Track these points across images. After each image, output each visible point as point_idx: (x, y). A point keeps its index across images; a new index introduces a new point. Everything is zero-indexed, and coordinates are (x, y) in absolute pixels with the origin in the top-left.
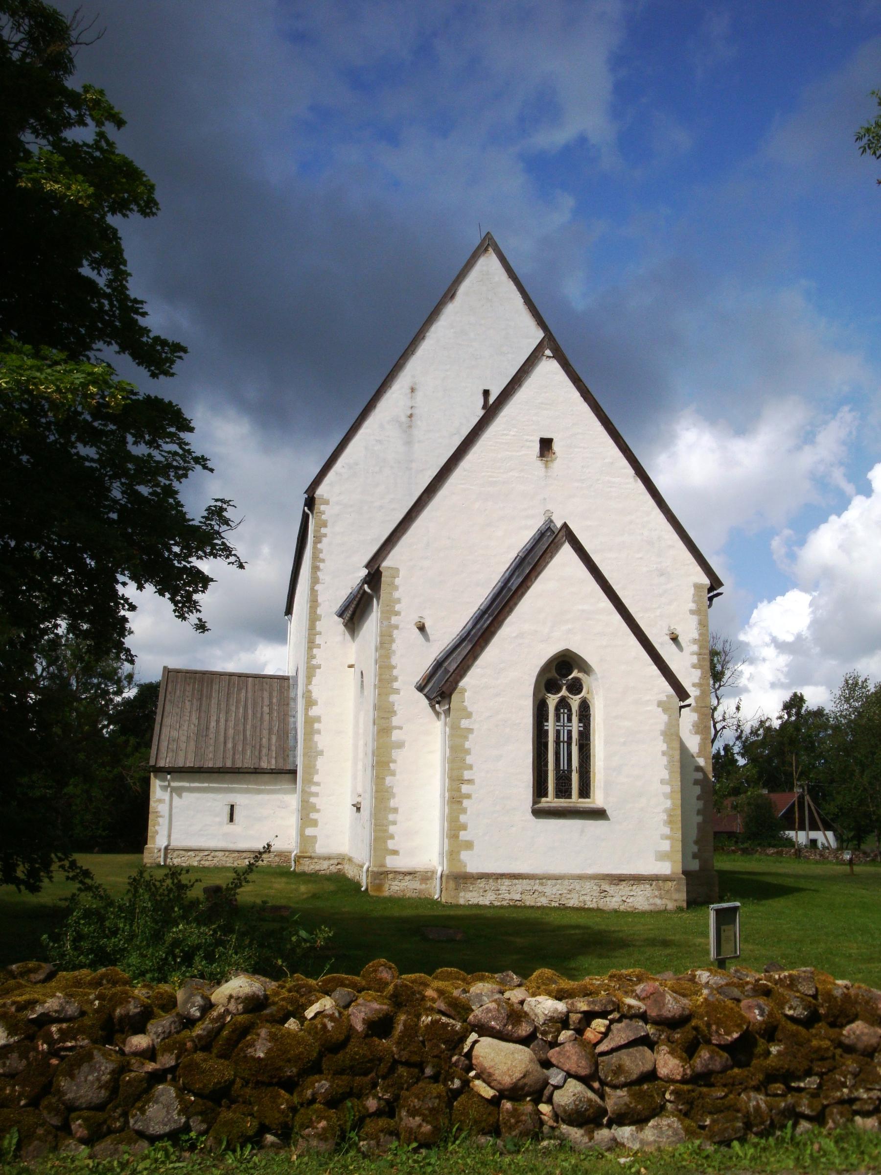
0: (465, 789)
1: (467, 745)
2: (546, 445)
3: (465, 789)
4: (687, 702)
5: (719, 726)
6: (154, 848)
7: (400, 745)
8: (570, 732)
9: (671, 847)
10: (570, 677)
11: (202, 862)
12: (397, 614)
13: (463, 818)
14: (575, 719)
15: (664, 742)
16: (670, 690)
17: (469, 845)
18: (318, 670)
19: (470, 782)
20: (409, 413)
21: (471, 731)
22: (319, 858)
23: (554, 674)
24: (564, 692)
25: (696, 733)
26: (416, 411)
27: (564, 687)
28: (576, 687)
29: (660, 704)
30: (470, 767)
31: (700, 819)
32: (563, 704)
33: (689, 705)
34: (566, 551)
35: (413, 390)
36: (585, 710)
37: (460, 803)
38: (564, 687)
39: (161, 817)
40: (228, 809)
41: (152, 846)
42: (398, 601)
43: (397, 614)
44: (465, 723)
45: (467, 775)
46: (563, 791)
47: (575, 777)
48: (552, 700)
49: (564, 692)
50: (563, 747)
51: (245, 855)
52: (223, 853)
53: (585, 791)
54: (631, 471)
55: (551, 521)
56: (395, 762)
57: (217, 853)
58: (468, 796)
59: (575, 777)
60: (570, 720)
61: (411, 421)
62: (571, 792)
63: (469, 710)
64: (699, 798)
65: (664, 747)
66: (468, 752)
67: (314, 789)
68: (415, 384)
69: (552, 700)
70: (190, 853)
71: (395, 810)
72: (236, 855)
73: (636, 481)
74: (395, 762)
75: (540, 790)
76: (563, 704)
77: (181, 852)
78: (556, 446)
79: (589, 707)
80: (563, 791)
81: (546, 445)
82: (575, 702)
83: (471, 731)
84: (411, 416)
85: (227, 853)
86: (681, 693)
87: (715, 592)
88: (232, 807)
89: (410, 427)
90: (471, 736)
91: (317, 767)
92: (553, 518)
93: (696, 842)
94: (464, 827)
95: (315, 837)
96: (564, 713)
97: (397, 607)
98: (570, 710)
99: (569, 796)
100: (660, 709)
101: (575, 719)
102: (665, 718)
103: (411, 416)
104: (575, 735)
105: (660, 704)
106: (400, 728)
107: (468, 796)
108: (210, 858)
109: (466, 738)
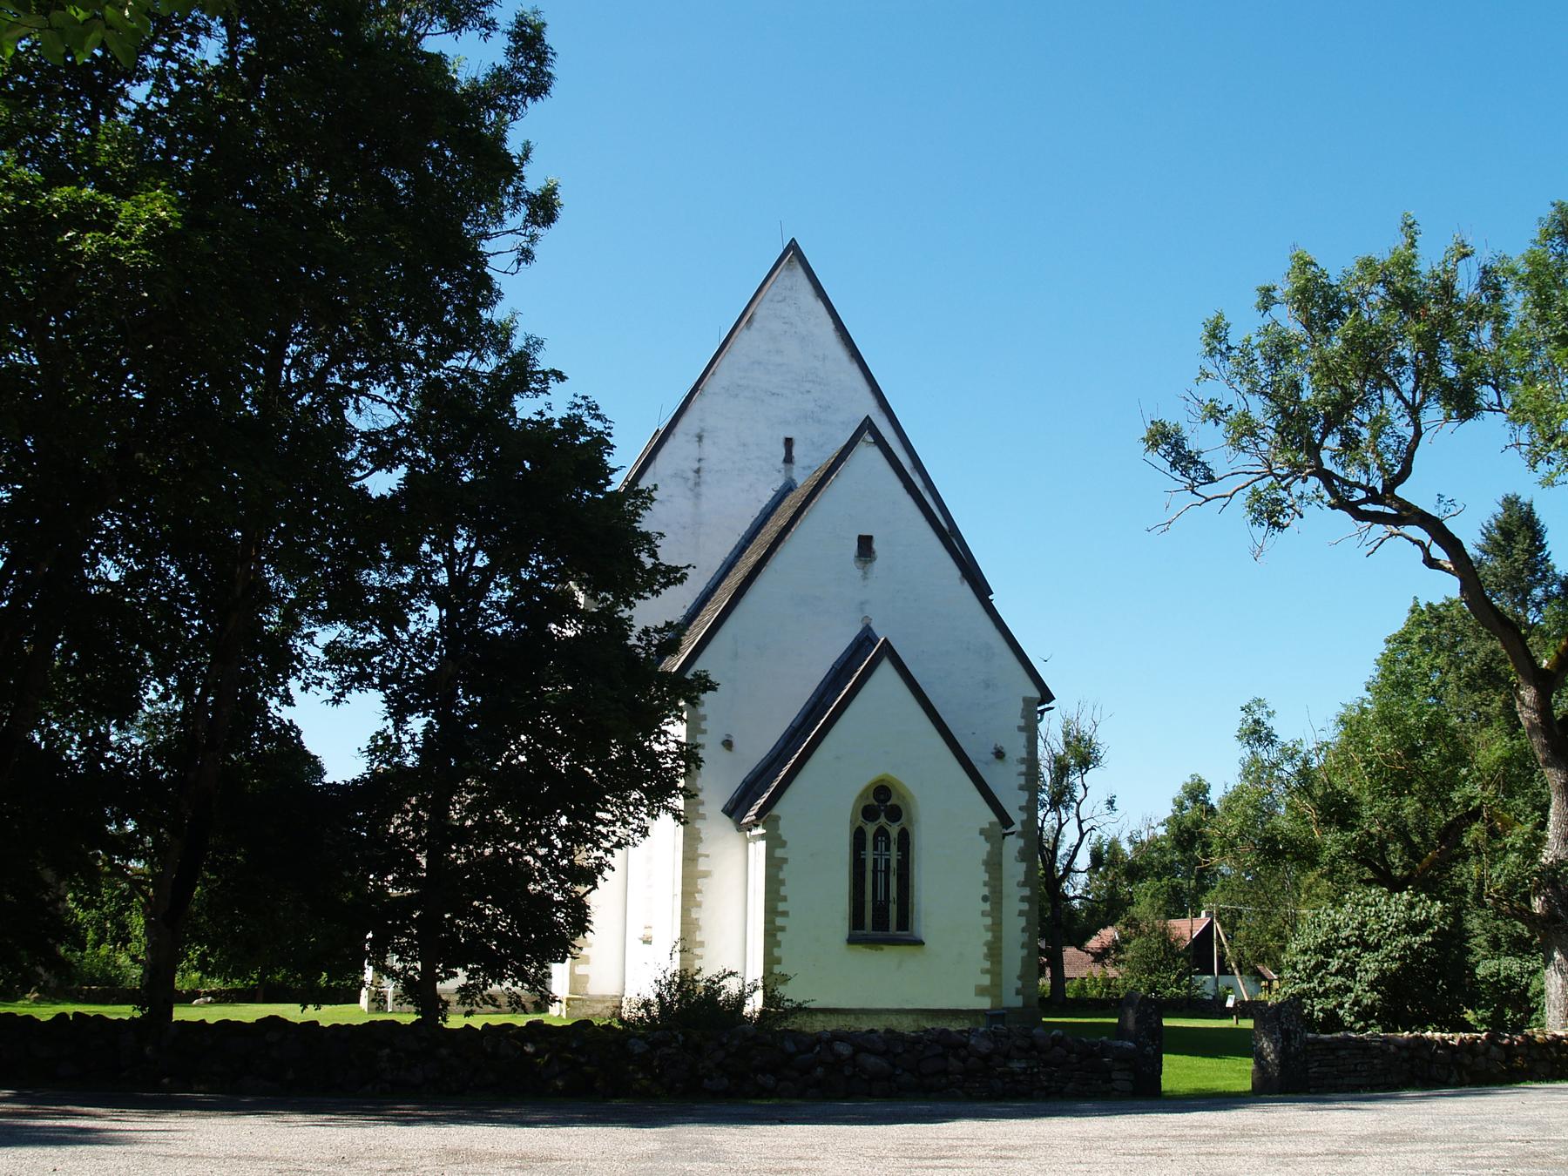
0: (779, 921)
1: (781, 876)
2: (865, 545)
3: (779, 921)
4: (1010, 830)
5: (1085, 827)
7: (706, 875)
8: (888, 861)
9: (992, 981)
10: (888, 804)
12: (704, 732)
13: (777, 952)
14: (894, 848)
15: (986, 871)
16: (994, 818)
17: (785, 979)
19: (785, 914)
20: (696, 466)
21: (785, 860)
22: (591, 1001)
23: (872, 801)
24: (882, 820)
25: (1022, 860)
26: (703, 464)
27: (883, 814)
28: (895, 814)
29: (982, 832)
30: (784, 899)
31: (1025, 952)
32: (882, 832)
33: (1013, 833)
34: (886, 669)
35: (700, 438)
36: (905, 840)
37: (775, 936)
38: (883, 814)
42: (704, 718)
43: (704, 732)
44: (779, 853)
45: (781, 907)
46: (881, 921)
47: (893, 909)
48: (870, 829)
49: (882, 820)
50: (881, 877)
53: (904, 921)
54: (955, 572)
55: (870, 629)
56: (700, 892)
58: (782, 929)
59: (893, 909)
60: (888, 848)
61: (699, 477)
62: (888, 925)
63: (784, 838)
64: (1023, 930)
65: (986, 877)
66: (782, 882)
68: (703, 430)
69: (870, 829)
71: (702, 944)
73: (962, 583)
74: (700, 892)
75: (857, 919)
76: (882, 832)
78: (875, 546)
79: (908, 834)
80: (881, 921)
81: (865, 545)
82: (894, 831)
83: (785, 860)
84: (698, 471)
86: (1005, 820)
87: (1046, 706)
89: (697, 484)
90: (785, 867)
92: (872, 625)
93: (1020, 978)
94: (778, 961)
96: (882, 841)
97: (704, 725)
98: (888, 838)
99: (887, 929)
100: (983, 837)
101: (894, 848)
102: (987, 847)
103: (698, 471)
104: (894, 864)
105: (982, 832)
106: (707, 856)
107: (782, 929)
109: (780, 868)
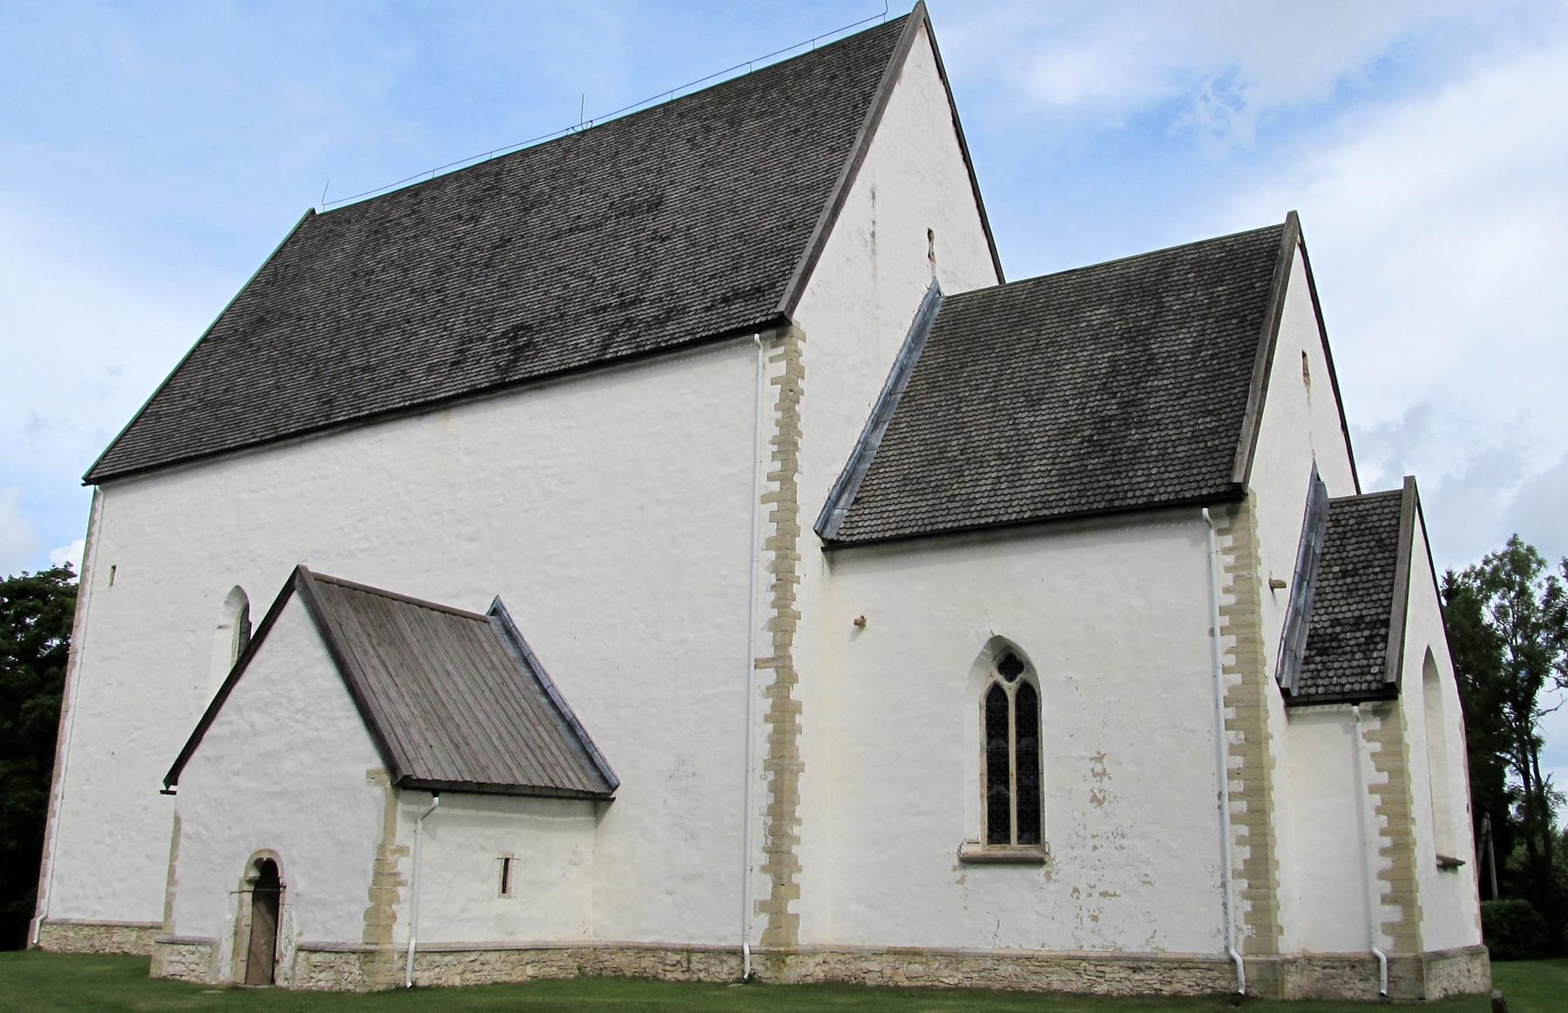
6: (393, 951)
11: (467, 976)
18: (797, 621)
39: (401, 884)
40: (500, 865)
41: (388, 947)
51: (527, 957)
52: (497, 955)
57: (488, 956)
67: (796, 830)
70: (449, 958)
72: (515, 957)
77: (437, 957)
85: (503, 955)
88: (507, 861)
91: (799, 792)
95: (797, 916)
108: (477, 966)
